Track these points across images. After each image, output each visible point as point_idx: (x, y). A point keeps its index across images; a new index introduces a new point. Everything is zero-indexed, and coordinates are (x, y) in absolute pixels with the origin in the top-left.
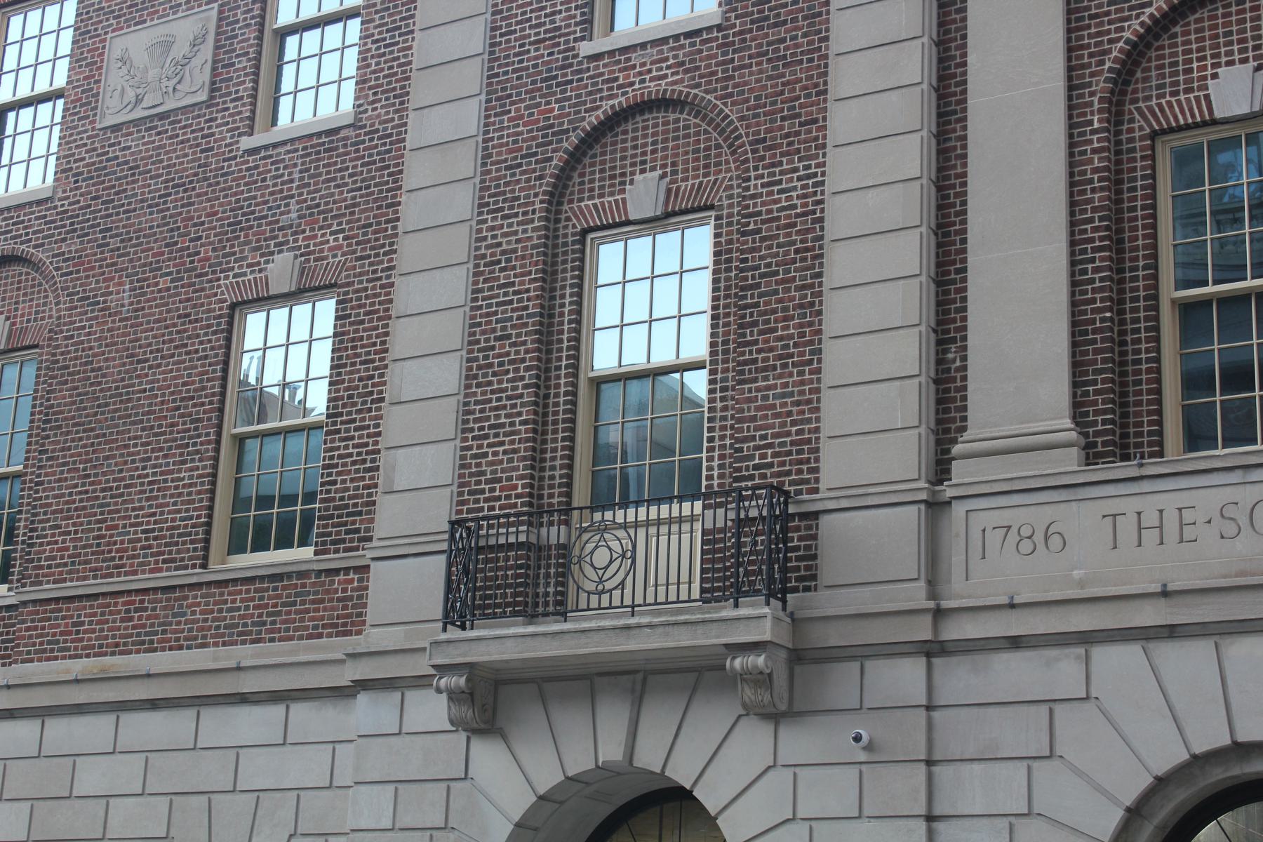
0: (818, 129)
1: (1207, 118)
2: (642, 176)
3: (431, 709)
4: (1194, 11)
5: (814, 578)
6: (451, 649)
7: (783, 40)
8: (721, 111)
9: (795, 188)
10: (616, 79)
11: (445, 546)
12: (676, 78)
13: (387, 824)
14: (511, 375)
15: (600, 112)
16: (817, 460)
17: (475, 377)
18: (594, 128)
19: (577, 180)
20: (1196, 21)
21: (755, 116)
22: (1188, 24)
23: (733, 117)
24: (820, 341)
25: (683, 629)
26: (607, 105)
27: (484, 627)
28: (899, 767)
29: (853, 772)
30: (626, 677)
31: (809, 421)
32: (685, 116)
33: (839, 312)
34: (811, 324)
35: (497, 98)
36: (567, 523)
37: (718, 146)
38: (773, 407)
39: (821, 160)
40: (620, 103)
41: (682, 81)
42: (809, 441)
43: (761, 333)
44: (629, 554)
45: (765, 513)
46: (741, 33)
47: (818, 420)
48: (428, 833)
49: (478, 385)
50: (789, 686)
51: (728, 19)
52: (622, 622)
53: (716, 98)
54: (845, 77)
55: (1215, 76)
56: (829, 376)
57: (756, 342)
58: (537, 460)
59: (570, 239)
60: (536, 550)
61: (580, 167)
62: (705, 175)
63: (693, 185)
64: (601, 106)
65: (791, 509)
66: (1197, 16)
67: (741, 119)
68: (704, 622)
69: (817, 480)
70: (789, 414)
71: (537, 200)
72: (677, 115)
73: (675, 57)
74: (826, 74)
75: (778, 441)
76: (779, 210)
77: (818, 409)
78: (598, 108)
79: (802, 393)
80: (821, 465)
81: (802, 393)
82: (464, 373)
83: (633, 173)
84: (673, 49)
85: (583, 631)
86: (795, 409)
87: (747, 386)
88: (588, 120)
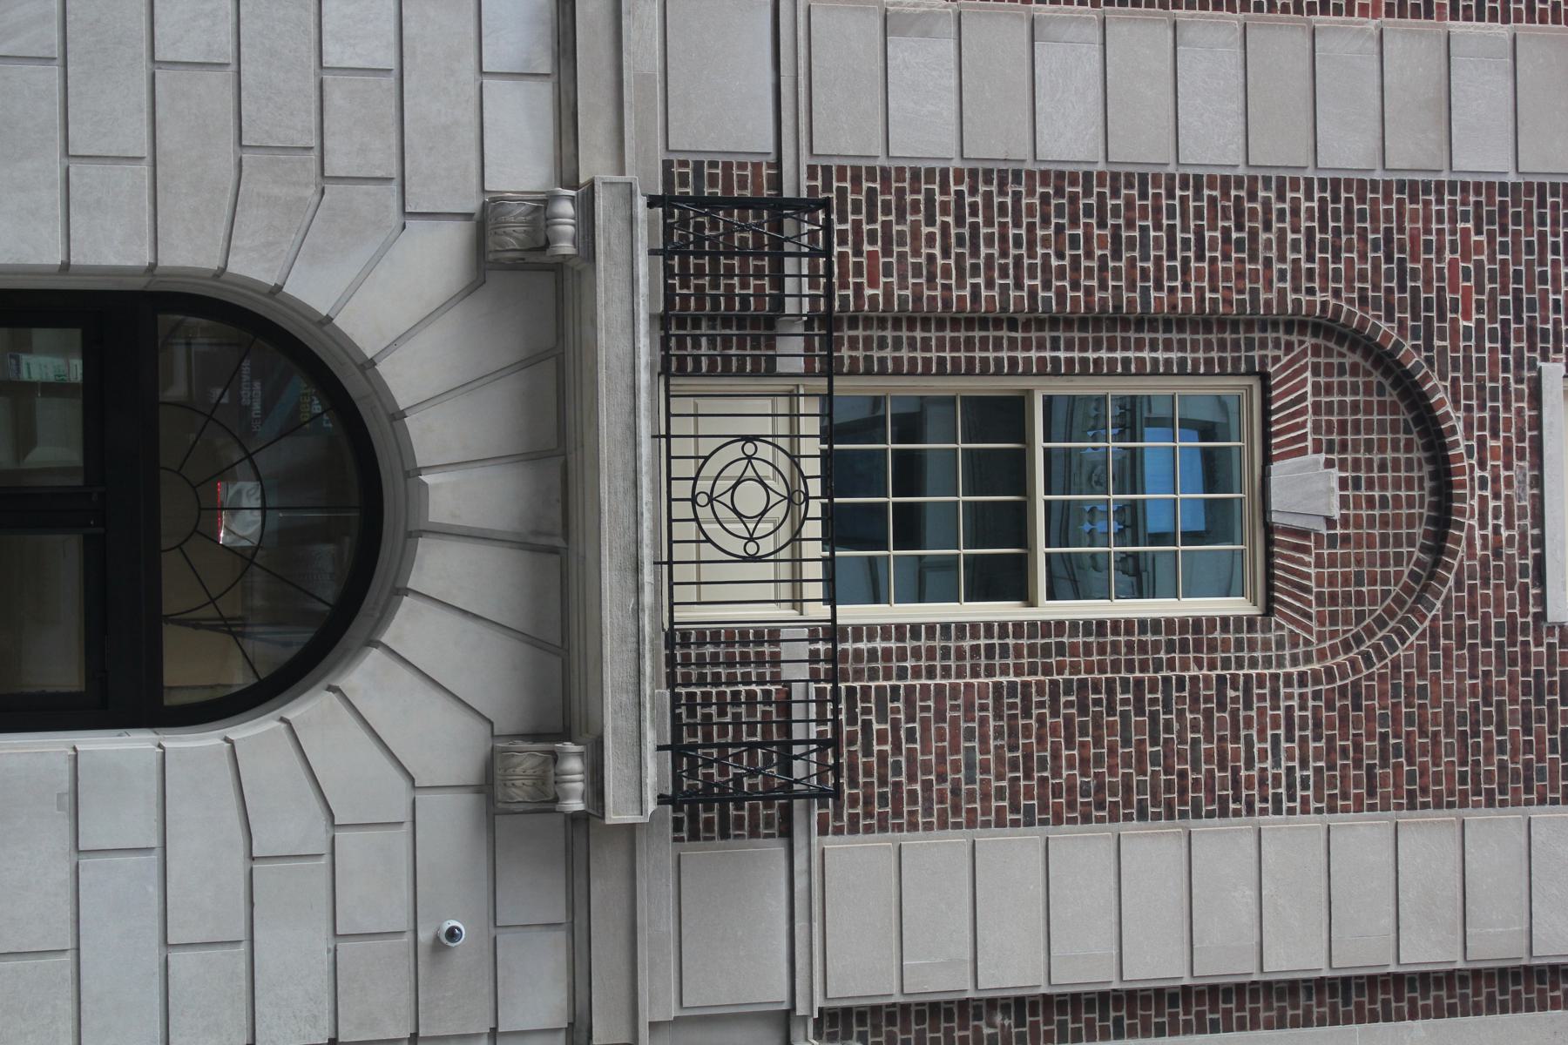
0: (1358, 798)
2: (1335, 484)
3: (520, 168)
5: (694, 836)
6: (620, 225)
7: (1501, 730)
8: (1413, 629)
9: (1277, 764)
10: (1495, 435)
11: (788, 192)
12: (1478, 542)
13: (329, 61)
14: (1054, 262)
15: (1449, 407)
16: (868, 829)
17: (1059, 192)
18: (1425, 397)
19: (1347, 361)
21: (1396, 687)
23: (1401, 652)
24: (1044, 822)
25: (631, 668)
26: (1457, 419)
27: (651, 223)
28: (407, 997)
29: (404, 923)
30: (558, 518)
31: (928, 812)
32: (1417, 554)
33: (1082, 850)
34: (1071, 805)
35: (1506, 204)
36: (809, 373)
37: (1360, 616)
38: (955, 749)
39: (1313, 805)
40: (1456, 444)
41: (1471, 556)
42: (898, 813)
43: (1069, 720)
44: (752, 548)
45: (796, 787)
46: (1526, 656)
47: (928, 827)
48: (314, 143)
49: (1045, 198)
50: (529, 806)
51: (1551, 630)
52: (647, 554)
53: (1435, 618)
54: (1428, 838)
56: (991, 840)
57: (1055, 713)
58: (914, 319)
59: (1256, 354)
60: (767, 324)
61: (1368, 365)
62: (1319, 596)
63: (1307, 576)
64: (1457, 408)
65: (797, 804)
67: (1396, 666)
68: (640, 705)
69: (838, 831)
70: (942, 778)
71: (1329, 297)
72: (1419, 541)
73: (1510, 539)
74: (1438, 805)
75: (903, 759)
76: (1249, 739)
77: (943, 825)
78: (1456, 403)
79: (971, 796)
80: (861, 836)
81: (971, 796)
82: (1067, 168)
83: (1343, 465)
84: (1523, 535)
85: (636, 484)
86: (948, 786)
87: (990, 702)
88: (1440, 384)
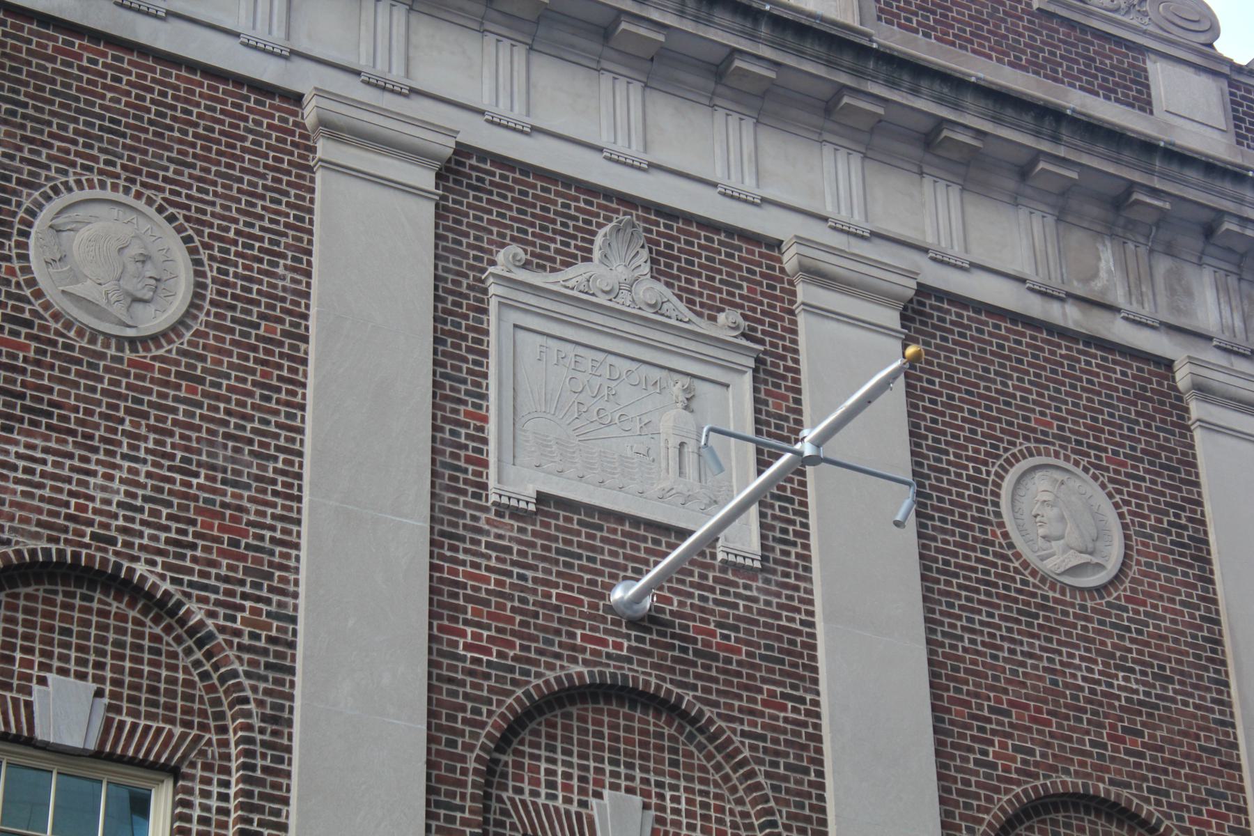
1: (25, 733)
4: (28, 585)
20: (28, 597)
22: (16, 596)
55: (42, 681)
66: (30, 590)
